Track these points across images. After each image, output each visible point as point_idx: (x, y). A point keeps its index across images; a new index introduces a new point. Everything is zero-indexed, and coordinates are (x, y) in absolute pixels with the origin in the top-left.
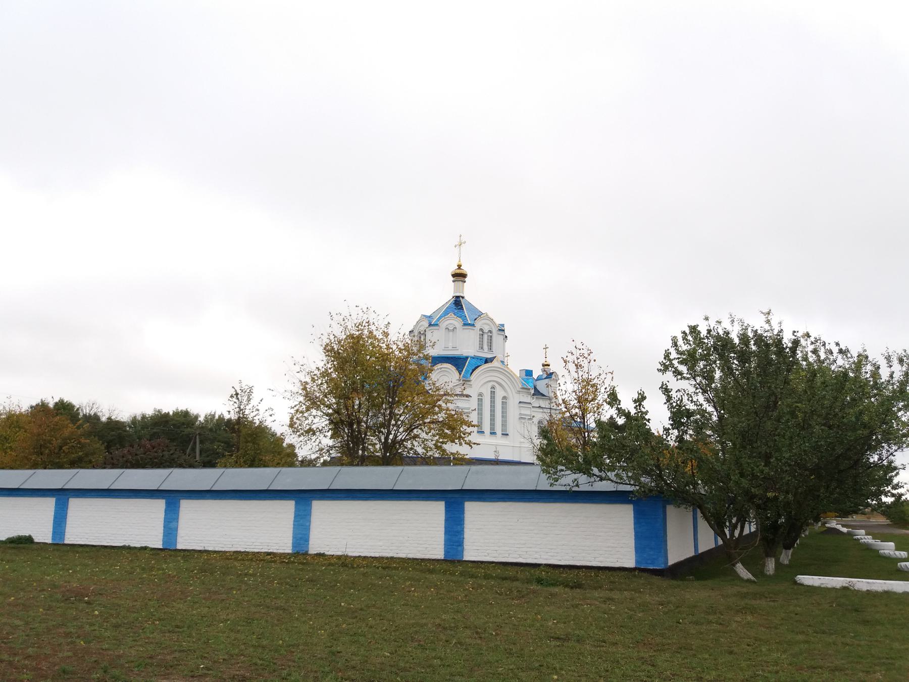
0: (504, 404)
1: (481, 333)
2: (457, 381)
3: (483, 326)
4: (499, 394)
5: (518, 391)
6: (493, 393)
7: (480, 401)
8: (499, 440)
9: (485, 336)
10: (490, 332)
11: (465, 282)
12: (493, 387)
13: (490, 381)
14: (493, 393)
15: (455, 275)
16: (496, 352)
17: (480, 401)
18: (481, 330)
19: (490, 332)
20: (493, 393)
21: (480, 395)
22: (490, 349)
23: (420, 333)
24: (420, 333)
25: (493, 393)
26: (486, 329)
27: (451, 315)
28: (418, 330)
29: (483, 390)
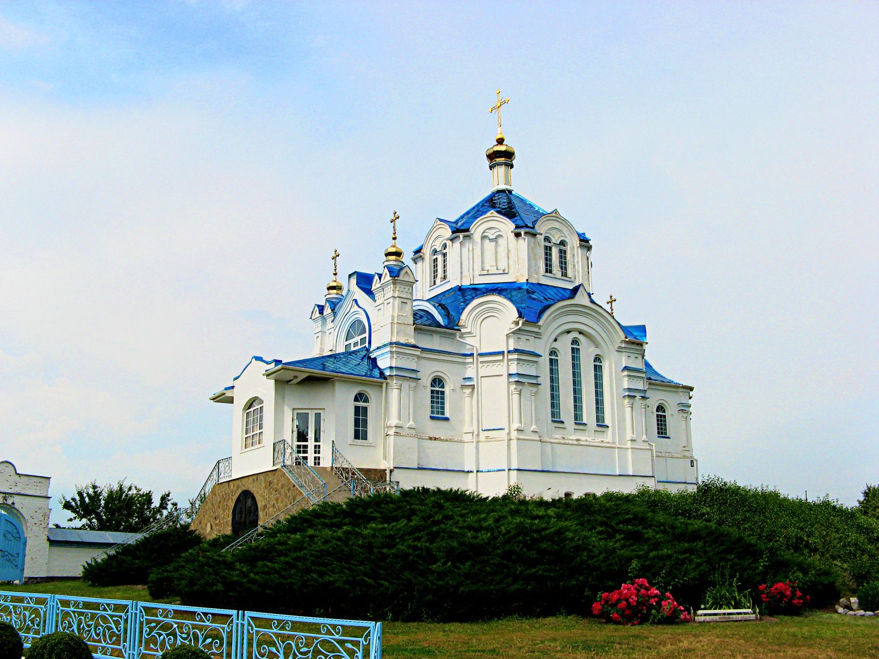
0: (598, 369)
2: (513, 326)
4: (587, 352)
5: (620, 347)
6: (575, 351)
7: (553, 362)
9: (555, 252)
10: (562, 243)
11: (512, 166)
12: (575, 341)
15: (492, 156)
16: (577, 273)
17: (553, 362)
18: (547, 239)
19: (562, 243)
20: (575, 351)
21: (553, 352)
22: (564, 274)
23: (435, 252)
24: (435, 252)
27: (492, 213)
28: (431, 247)
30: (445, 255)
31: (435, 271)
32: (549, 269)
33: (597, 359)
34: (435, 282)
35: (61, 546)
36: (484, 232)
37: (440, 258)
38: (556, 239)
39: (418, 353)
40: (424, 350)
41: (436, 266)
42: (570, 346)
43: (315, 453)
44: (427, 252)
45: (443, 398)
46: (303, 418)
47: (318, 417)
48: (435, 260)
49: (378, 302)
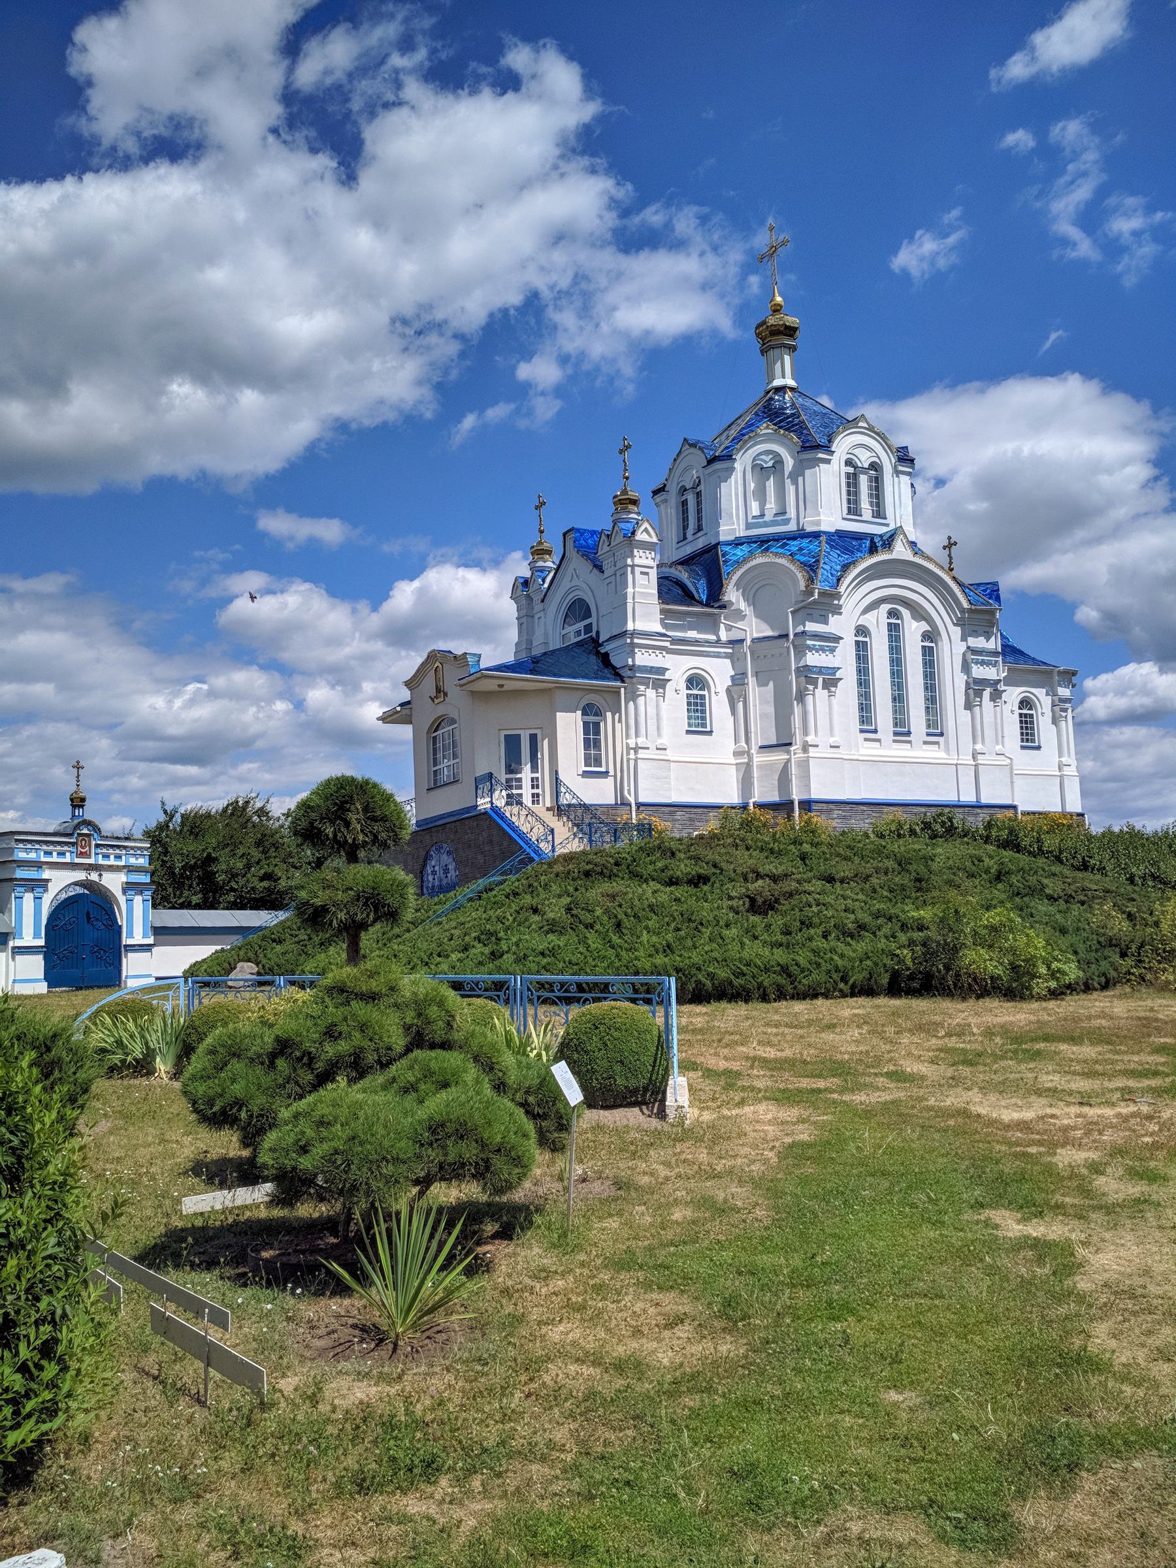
0: (928, 652)
1: (851, 470)
3: (856, 451)
4: (913, 630)
8: (918, 751)
9: (863, 480)
10: (875, 467)
12: (892, 613)
13: (883, 600)
14: (894, 631)
19: (875, 467)
21: (861, 630)
23: (683, 490)
24: (683, 490)
25: (894, 631)
26: (864, 458)
29: (869, 620)
30: (699, 494)
31: (685, 519)
32: (854, 509)
33: (926, 636)
34: (685, 534)
35: (174, 934)
36: (754, 460)
37: (691, 498)
38: (864, 458)
39: (667, 644)
40: (675, 641)
41: (685, 511)
42: (884, 621)
43: (533, 787)
44: (673, 488)
45: (703, 705)
46: (512, 743)
47: (533, 739)
48: (684, 503)
49: (606, 574)
